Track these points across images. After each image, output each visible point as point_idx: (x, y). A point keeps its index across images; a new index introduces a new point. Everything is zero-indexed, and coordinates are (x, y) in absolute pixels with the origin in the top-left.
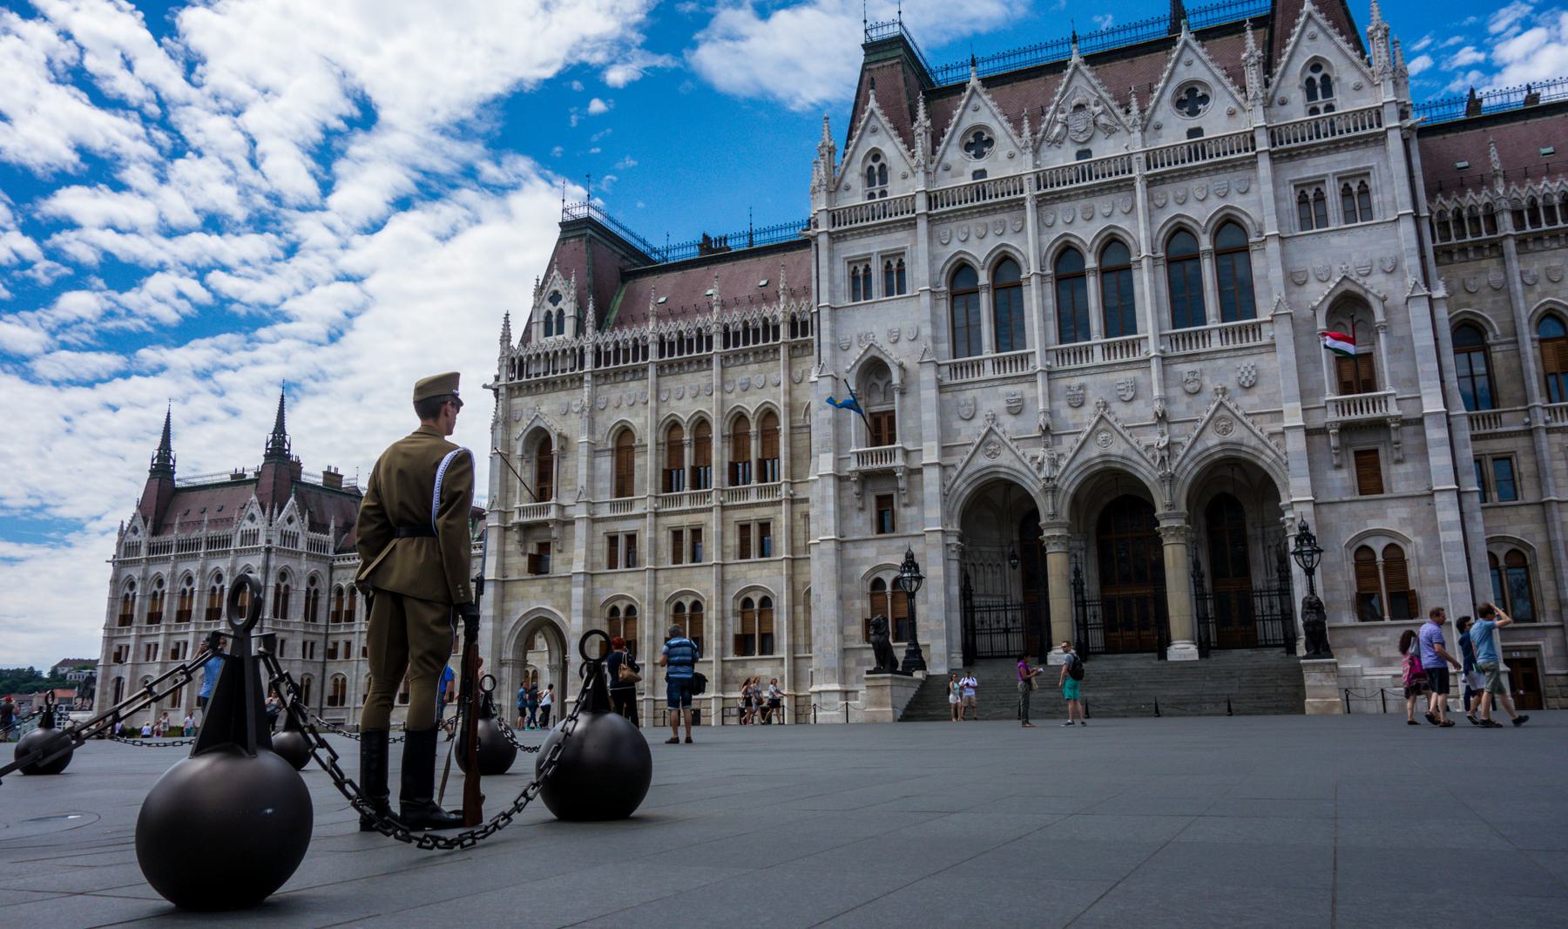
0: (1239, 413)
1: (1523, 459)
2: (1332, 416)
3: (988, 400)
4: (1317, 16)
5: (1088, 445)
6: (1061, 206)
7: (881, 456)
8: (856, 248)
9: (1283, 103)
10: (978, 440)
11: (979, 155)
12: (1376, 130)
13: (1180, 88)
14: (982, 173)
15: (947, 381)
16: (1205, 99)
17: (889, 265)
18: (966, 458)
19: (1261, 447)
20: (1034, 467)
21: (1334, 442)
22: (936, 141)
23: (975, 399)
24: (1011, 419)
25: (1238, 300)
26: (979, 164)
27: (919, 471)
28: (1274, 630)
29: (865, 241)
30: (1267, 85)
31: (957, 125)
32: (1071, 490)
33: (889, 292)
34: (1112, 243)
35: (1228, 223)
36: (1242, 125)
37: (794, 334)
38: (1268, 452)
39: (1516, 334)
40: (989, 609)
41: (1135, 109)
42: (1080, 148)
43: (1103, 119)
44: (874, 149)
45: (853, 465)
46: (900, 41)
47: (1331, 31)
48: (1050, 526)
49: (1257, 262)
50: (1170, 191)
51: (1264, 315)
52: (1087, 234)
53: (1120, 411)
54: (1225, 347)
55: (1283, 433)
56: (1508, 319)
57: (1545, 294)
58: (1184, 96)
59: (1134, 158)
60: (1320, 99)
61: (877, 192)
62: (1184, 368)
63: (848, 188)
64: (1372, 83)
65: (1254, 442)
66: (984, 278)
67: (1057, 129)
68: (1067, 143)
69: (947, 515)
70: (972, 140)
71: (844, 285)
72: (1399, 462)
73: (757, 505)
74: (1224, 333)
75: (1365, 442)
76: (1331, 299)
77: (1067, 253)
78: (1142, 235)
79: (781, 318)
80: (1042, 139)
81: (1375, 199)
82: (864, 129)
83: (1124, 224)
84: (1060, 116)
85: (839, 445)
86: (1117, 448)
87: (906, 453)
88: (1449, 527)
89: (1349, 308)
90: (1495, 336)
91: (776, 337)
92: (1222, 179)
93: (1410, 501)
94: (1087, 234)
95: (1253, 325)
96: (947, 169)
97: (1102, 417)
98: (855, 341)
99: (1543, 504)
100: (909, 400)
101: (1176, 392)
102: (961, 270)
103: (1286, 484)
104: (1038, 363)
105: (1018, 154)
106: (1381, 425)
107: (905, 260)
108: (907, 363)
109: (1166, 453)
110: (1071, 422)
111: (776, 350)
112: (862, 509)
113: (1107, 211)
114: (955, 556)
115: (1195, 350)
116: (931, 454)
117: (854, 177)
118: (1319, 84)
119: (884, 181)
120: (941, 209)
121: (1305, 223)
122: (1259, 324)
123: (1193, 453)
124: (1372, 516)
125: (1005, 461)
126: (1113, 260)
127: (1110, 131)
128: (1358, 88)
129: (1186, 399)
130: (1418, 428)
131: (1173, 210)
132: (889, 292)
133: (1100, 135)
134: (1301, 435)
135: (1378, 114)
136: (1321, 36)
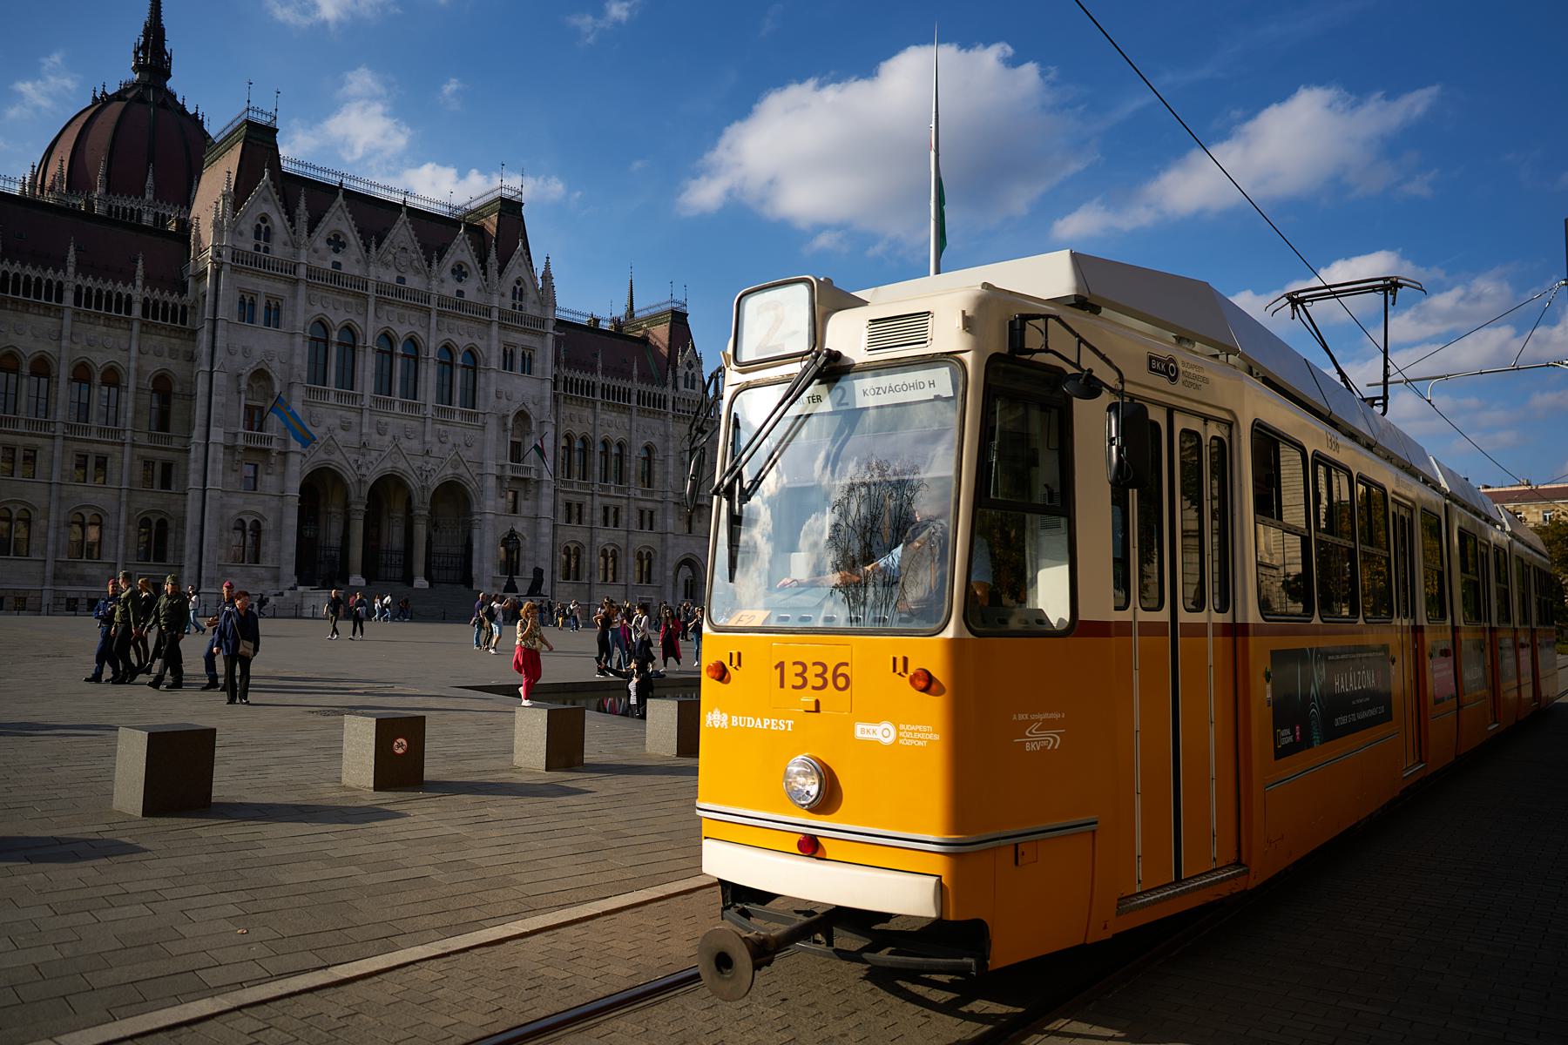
2: (509, 473)
7: (260, 439)
11: (336, 251)
16: (466, 275)
25: (471, 399)
26: (338, 258)
29: (254, 280)
35: (471, 353)
49: (481, 380)
52: (401, 331)
75: (515, 486)
77: (387, 337)
78: (432, 346)
86: (402, 465)
89: (522, 416)
101: (435, 440)
104: (367, 402)
118: (518, 294)
125: (337, 457)
127: (417, 272)
131: (447, 335)
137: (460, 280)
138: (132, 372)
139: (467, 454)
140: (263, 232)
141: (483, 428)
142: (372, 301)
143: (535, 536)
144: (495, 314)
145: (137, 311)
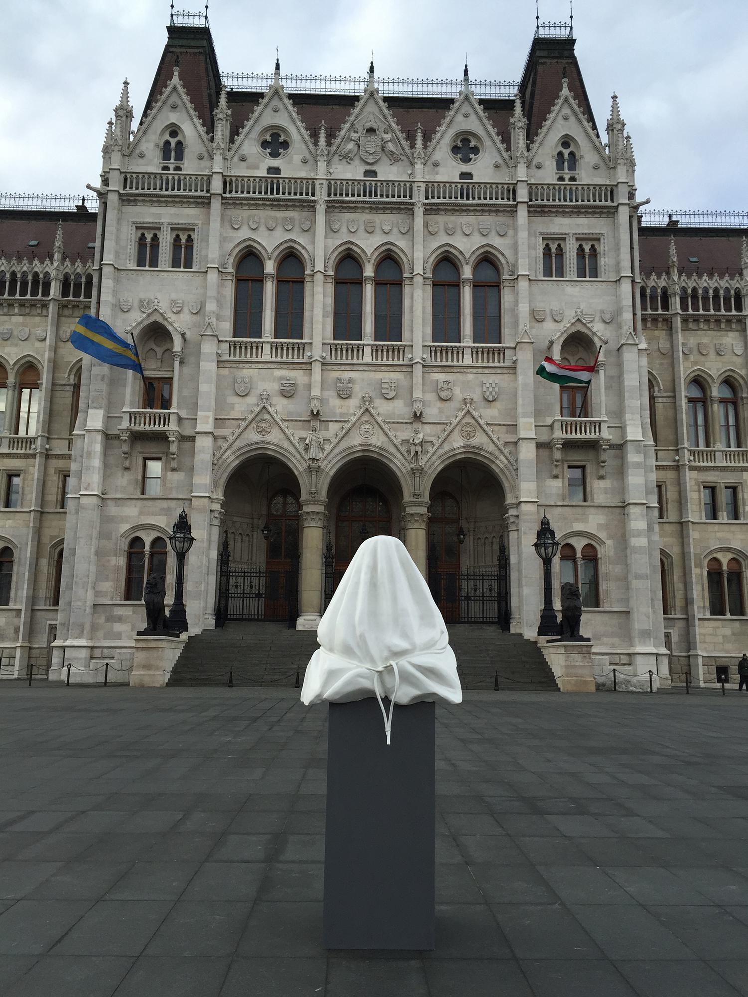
0: (482, 422)
1: (670, 487)
2: (558, 434)
3: (264, 379)
4: (572, 101)
5: (351, 433)
6: (347, 216)
7: (154, 419)
8: (148, 214)
9: (539, 167)
10: (250, 417)
11: (275, 154)
12: (609, 203)
13: (457, 135)
14: (277, 170)
15: (226, 357)
16: (476, 150)
17: (177, 239)
18: (238, 432)
19: (497, 453)
20: (301, 447)
21: (557, 455)
22: (235, 131)
23: (251, 378)
24: (285, 401)
25: (489, 327)
26: (275, 163)
27: (192, 439)
28: (492, 610)
29: (154, 210)
30: (528, 150)
31: (256, 121)
32: (332, 473)
33: (175, 263)
34: (389, 259)
35: (487, 260)
36: (503, 178)
37: (65, 293)
38: (502, 457)
39: (674, 391)
40: (244, 574)
41: (419, 142)
42: (368, 168)
43: (391, 146)
44: (173, 124)
45: (125, 424)
46: (203, 35)
47: (581, 116)
48: (308, 503)
49: (507, 297)
50: (441, 220)
51: (507, 342)
52: (369, 246)
53: (382, 408)
54: (475, 364)
55: (516, 443)
56: (670, 379)
57: (696, 363)
58: (460, 144)
59: (415, 185)
60: (567, 171)
61: (171, 166)
62: (441, 377)
63: (141, 156)
64: (608, 166)
65: (491, 448)
66: (270, 267)
67: (351, 146)
68: (357, 161)
69: (216, 484)
70: (269, 139)
71: (132, 250)
72: (602, 477)
73: (8, 456)
74: (475, 352)
75: (577, 457)
76: (565, 336)
77: (348, 259)
78: (419, 257)
79: (53, 274)
80: (335, 153)
81: (602, 261)
82: (164, 102)
83: (402, 243)
84: (354, 136)
85: (111, 407)
86: (377, 440)
87: (180, 419)
88: (639, 534)
89: (579, 342)
90: (659, 390)
91: (46, 292)
92: (488, 220)
93: (607, 509)
94: (369, 246)
95: (499, 349)
96: (243, 159)
97: (367, 410)
98: (136, 304)
99: (681, 523)
100: (186, 370)
101: (431, 397)
102: (249, 257)
103: (515, 487)
105: (311, 161)
106: (593, 445)
107: (195, 236)
108: (188, 335)
109: (419, 448)
110: (338, 411)
111: (45, 306)
112: (127, 469)
113: (387, 228)
114: (217, 522)
115: (450, 363)
116: (205, 422)
117: (150, 146)
118: (567, 158)
119: (179, 156)
120: (236, 194)
121: (548, 272)
122: (504, 349)
123: (441, 451)
124: (577, 520)
125: (274, 437)
126: (389, 275)
127: (394, 158)
128: (596, 168)
129: (439, 404)
130: (618, 451)
131: (446, 239)
132: (175, 263)
133: (385, 159)
134: (533, 445)
135: (612, 192)
136: (573, 119)
137: (466, 160)
138: (46, 365)
139: (489, 414)
140: (173, 149)
141: (513, 369)
142: (321, 208)
143: (623, 539)
144: (522, 194)
145: (55, 290)
